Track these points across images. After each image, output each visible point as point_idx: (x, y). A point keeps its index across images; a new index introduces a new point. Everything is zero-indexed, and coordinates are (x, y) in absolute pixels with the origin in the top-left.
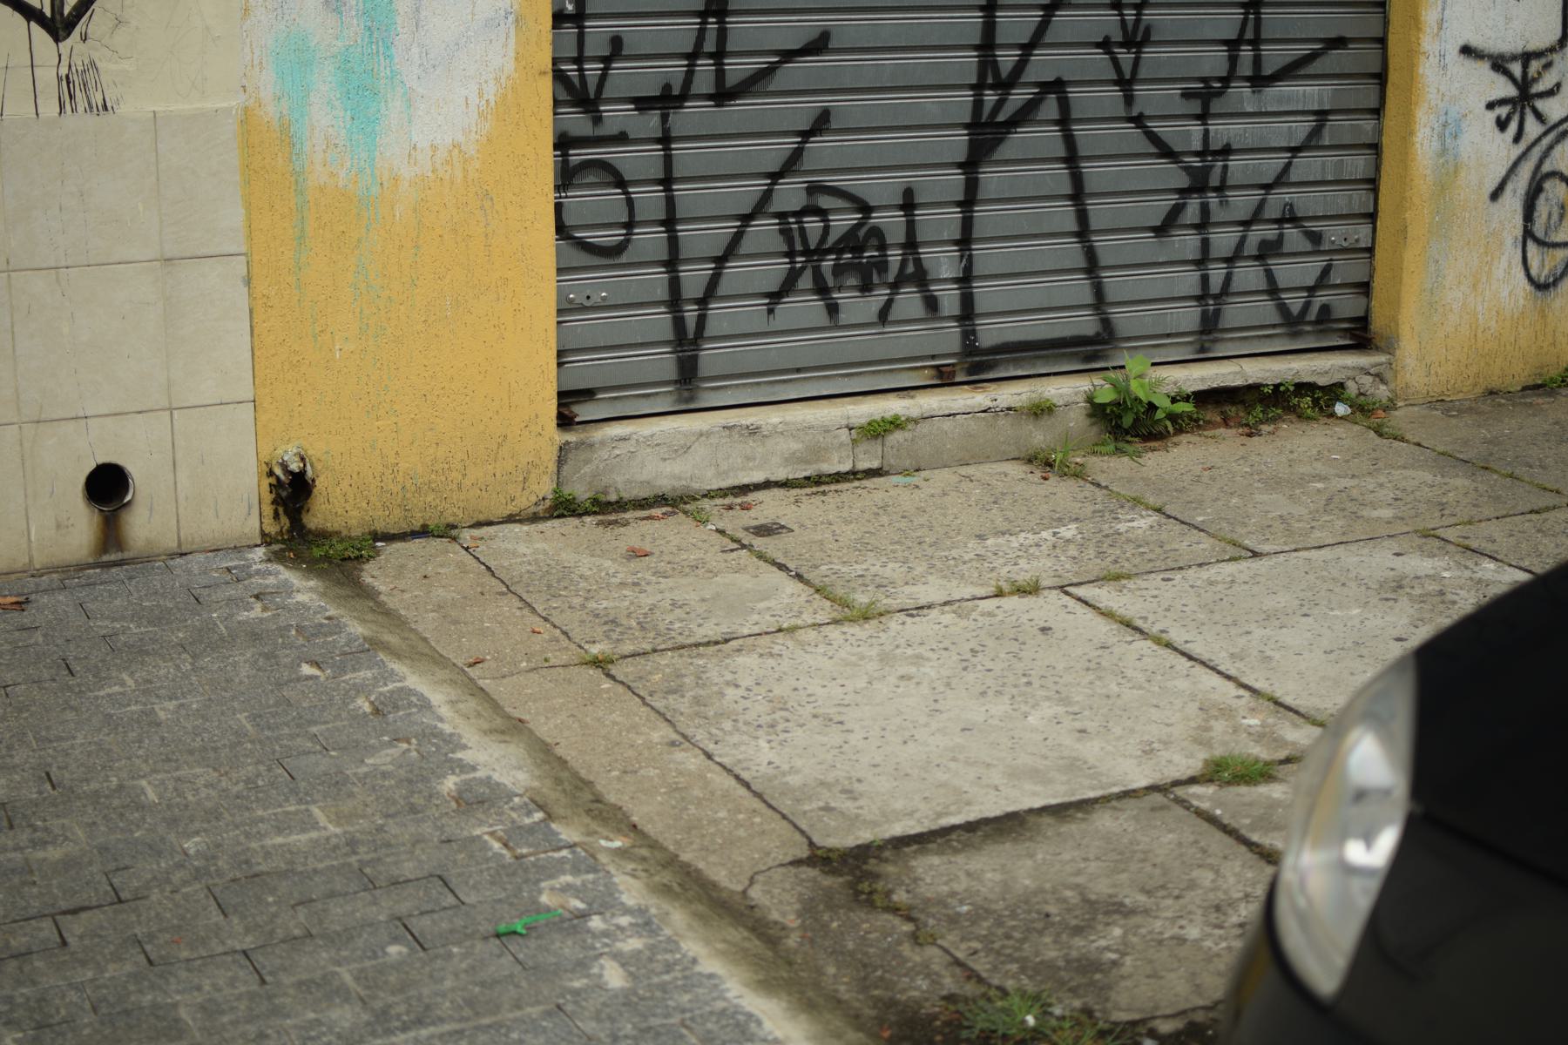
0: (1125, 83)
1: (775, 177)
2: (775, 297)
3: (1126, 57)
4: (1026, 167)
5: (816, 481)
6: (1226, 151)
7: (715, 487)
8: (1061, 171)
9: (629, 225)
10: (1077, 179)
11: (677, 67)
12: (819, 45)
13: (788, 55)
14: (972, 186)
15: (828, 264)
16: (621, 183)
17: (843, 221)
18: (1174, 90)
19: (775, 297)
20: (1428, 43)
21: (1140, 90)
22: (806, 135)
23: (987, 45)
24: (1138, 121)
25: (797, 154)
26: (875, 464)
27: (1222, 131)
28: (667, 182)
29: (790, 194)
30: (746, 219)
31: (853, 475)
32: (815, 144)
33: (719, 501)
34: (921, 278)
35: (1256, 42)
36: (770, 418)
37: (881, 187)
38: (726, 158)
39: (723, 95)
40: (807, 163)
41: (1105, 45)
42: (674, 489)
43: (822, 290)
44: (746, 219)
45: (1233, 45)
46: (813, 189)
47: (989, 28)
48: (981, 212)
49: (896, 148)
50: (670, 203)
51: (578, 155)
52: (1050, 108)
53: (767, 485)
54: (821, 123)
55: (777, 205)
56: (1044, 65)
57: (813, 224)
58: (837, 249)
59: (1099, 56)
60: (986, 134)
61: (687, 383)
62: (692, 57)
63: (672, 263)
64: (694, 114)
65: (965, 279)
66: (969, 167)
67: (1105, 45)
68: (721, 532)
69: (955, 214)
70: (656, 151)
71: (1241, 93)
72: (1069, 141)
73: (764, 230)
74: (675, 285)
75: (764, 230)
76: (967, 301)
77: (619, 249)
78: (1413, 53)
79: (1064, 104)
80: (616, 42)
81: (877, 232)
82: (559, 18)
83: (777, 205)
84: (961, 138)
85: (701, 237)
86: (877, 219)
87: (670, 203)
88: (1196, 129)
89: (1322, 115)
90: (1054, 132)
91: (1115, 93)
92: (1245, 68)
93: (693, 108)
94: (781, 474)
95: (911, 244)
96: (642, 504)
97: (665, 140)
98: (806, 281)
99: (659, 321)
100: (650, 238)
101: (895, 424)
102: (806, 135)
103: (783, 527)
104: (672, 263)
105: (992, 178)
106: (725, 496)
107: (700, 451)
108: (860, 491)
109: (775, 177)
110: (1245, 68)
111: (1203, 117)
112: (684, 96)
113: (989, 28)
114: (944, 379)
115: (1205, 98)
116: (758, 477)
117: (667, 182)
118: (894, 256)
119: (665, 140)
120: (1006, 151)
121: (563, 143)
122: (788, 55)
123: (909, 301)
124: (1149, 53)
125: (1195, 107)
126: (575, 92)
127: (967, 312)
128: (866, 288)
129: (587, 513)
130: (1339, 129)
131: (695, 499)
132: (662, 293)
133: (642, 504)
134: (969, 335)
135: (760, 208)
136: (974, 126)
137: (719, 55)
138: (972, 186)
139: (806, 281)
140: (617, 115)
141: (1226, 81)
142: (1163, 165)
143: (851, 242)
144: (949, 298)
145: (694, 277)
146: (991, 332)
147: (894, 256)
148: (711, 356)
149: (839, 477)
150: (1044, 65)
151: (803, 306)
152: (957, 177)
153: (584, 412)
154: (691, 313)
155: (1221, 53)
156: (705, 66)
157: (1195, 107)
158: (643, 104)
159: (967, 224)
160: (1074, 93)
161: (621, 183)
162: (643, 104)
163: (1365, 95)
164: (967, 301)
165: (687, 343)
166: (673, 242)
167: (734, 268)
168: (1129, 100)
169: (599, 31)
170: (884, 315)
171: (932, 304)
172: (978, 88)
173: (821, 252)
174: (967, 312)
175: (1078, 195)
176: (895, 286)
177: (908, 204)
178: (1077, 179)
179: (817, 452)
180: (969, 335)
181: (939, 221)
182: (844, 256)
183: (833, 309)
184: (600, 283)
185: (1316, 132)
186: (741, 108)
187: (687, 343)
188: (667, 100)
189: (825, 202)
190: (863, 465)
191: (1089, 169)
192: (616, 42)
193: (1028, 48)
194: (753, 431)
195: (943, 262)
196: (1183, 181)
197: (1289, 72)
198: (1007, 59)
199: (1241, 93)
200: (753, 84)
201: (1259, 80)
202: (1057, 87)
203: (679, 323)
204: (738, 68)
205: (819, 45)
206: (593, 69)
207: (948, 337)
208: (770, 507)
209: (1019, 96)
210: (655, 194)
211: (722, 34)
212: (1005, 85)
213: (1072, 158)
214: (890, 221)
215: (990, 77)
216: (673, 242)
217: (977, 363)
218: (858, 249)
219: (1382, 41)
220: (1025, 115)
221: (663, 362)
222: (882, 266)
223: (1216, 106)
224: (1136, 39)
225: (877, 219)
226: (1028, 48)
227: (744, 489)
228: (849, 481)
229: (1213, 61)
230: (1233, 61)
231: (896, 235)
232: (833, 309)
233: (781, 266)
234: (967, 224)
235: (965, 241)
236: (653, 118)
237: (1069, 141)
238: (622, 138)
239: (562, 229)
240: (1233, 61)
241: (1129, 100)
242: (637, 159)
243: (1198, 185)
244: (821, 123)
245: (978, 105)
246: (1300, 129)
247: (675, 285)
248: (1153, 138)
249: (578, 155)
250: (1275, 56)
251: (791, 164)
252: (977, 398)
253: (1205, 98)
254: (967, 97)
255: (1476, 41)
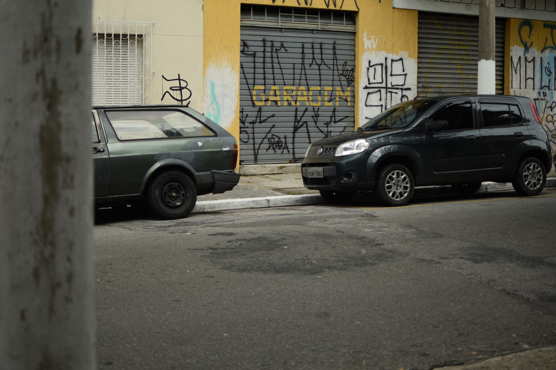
0: (316, 122)
1: (267, 133)
2: (267, 149)
3: (316, 118)
4: (302, 133)
5: (273, 174)
6: (331, 132)
8: (307, 134)
9: (248, 139)
10: (309, 135)
11: (255, 118)
12: (273, 116)
13: (269, 117)
14: (294, 136)
15: (274, 145)
16: (247, 133)
17: (276, 140)
18: (323, 123)
19: (267, 149)
20: (360, 117)
21: (318, 123)
22: (271, 128)
23: (296, 117)
24: (318, 127)
25: (270, 130)
27: (330, 129)
28: (253, 133)
29: (269, 136)
30: (264, 139)
31: (278, 174)
32: (273, 129)
34: (287, 148)
35: (335, 117)
36: (267, 165)
37: (282, 135)
38: (261, 130)
39: (260, 122)
40: (272, 131)
41: (312, 117)
43: (274, 149)
44: (264, 139)
45: (331, 117)
46: (272, 135)
47: (296, 114)
48: (295, 139)
49: (284, 130)
50: (254, 136)
51: (242, 129)
52: (305, 125)
54: (273, 126)
55: (268, 137)
56: (304, 119)
57: (272, 140)
58: (276, 143)
59: (311, 118)
60: (296, 129)
61: (256, 161)
62: (257, 117)
63: (254, 144)
64: (257, 125)
65: (293, 148)
66: (294, 133)
67: (312, 117)
69: (292, 139)
70: (252, 129)
71: (333, 124)
72: (308, 130)
73: (266, 140)
74: (254, 147)
75: (266, 140)
76: (294, 151)
77: (247, 142)
78: (358, 118)
79: (307, 125)
80: (247, 115)
81: (281, 141)
82: (240, 112)
83: (268, 137)
84: (293, 129)
85: (258, 141)
86: (281, 139)
87: (254, 136)
88: (326, 129)
89: (345, 127)
90: (305, 128)
91: (314, 123)
92: (333, 120)
93: (256, 124)
94: (268, 173)
95: (286, 143)
96: (250, 175)
97: (253, 128)
98: (271, 148)
99: (252, 152)
100: (251, 141)
101: (284, 167)
102: (271, 128)
104: (254, 144)
105: (297, 135)
107: (258, 169)
109: (267, 133)
110: (333, 120)
111: (327, 127)
112: (256, 122)
113: (296, 114)
114: (291, 162)
115: (327, 124)
116: (265, 173)
117: (253, 133)
118: (284, 145)
119: (253, 128)
120: (299, 131)
121: (240, 128)
122: (269, 117)
123: (286, 151)
124: (319, 118)
125: (326, 126)
126: (242, 122)
127: (294, 153)
128: (280, 149)
130: (348, 129)
132: (253, 148)
133: (250, 175)
134: (294, 156)
135: (265, 138)
136: (294, 127)
137: (260, 117)
138: (294, 136)
139: (271, 148)
140: (247, 124)
141: (330, 122)
142: (321, 133)
143: (278, 143)
144: (291, 151)
145: (257, 146)
146: (297, 156)
147: (284, 145)
148: (259, 157)
149: (276, 174)
150: (304, 119)
151: (271, 151)
152: (292, 134)
153: (242, 163)
154: (256, 151)
155: (329, 118)
156: (258, 118)
157: (326, 126)
158: (250, 123)
159: (293, 141)
160: (308, 123)
161: (247, 133)
162: (250, 123)
163: (352, 124)
164: (294, 151)
165: (256, 155)
166: (254, 141)
167: (262, 145)
168: (316, 124)
169: (245, 113)
170: (282, 153)
171: (289, 151)
172: (295, 122)
173: (274, 144)
174: (294, 153)
175: (309, 137)
176: (284, 149)
177: (285, 138)
178: (309, 135)
179: (273, 170)
180: (294, 156)
181: (290, 140)
182: (277, 144)
183: (275, 151)
184: (245, 147)
185: (344, 129)
186: (263, 124)
187: (256, 155)
188: (253, 123)
189: (274, 137)
191: (310, 134)
192: (247, 115)
193: (302, 117)
194: (265, 167)
195: (290, 146)
196: (324, 136)
197: (339, 121)
198: (299, 118)
199: (333, 124)
200: (264, 121)
201: (335, 122)
202: (306, 122)
203: (255, 152)
204: (262, 119)
205: (273, 116)
206: (244, 118)
207: (291, 156)
208: (267, 176)
209: (300, 123)
210: (252, 135)
211: (260, 114)
212: (299, 122)
213: (308, 132)
214: (283, 140)
215: (296, 121)
216: (254, 141)
217: (295, 160)
218: (279, 144)
219: (354, 117)
220: (301, 126)
221: (253, 157)
222: (282, 146)
223: (329, 125)
224: (317, 116)
225: (281, 139)
226: (302, 117)
229: (328, 119)
230: (331, 119)
231: (284, 142)
232: (275, 151)
233: (268, 145)
234: (293, 141)
235: (293, 143)
236: (251, 126)
237: (308, 130)
238: (247, 127)
239: (240, 139)
240: (331, 119)
241: (316, 124)
242: (250, 130)
243: (327, 136)
244: (273, 126)
245: (295, 124)
246: (342, 129)
247: (254, 147)
248: (320, 130)
249: (242, 129)
250: (337, 119)
251: (269, 132)
252: (296, 164)
253: (327, 124)
254: (293, 123)
255: (367, 117)
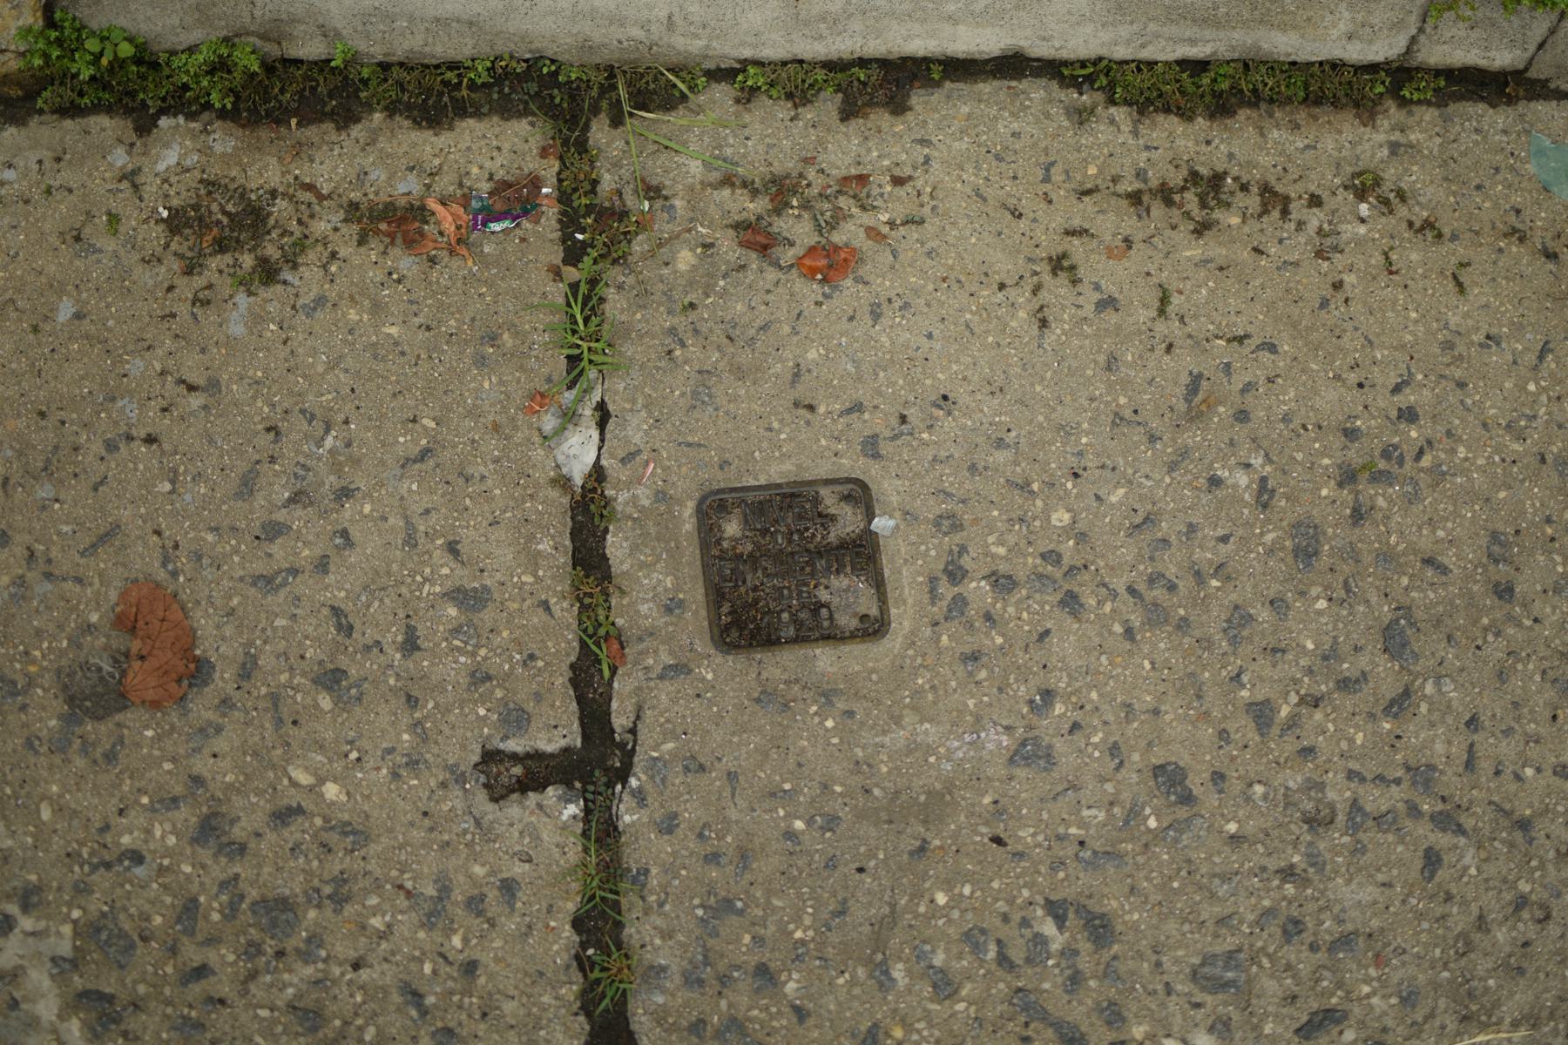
7: (774, 49)
26: (1503, 58)
33: (772, 137)
42: (586, 46)
53: (1012, 66)
68: (588, 511)
96: (435, 92)
103: (862, 553)
106: (799, 96)
108: (1361, 225)
129: (182, 102)
131: (669, 100)
133: (435, 92)
190: (1455, 47)
227: (888, 83)
228: (1366, 109)
